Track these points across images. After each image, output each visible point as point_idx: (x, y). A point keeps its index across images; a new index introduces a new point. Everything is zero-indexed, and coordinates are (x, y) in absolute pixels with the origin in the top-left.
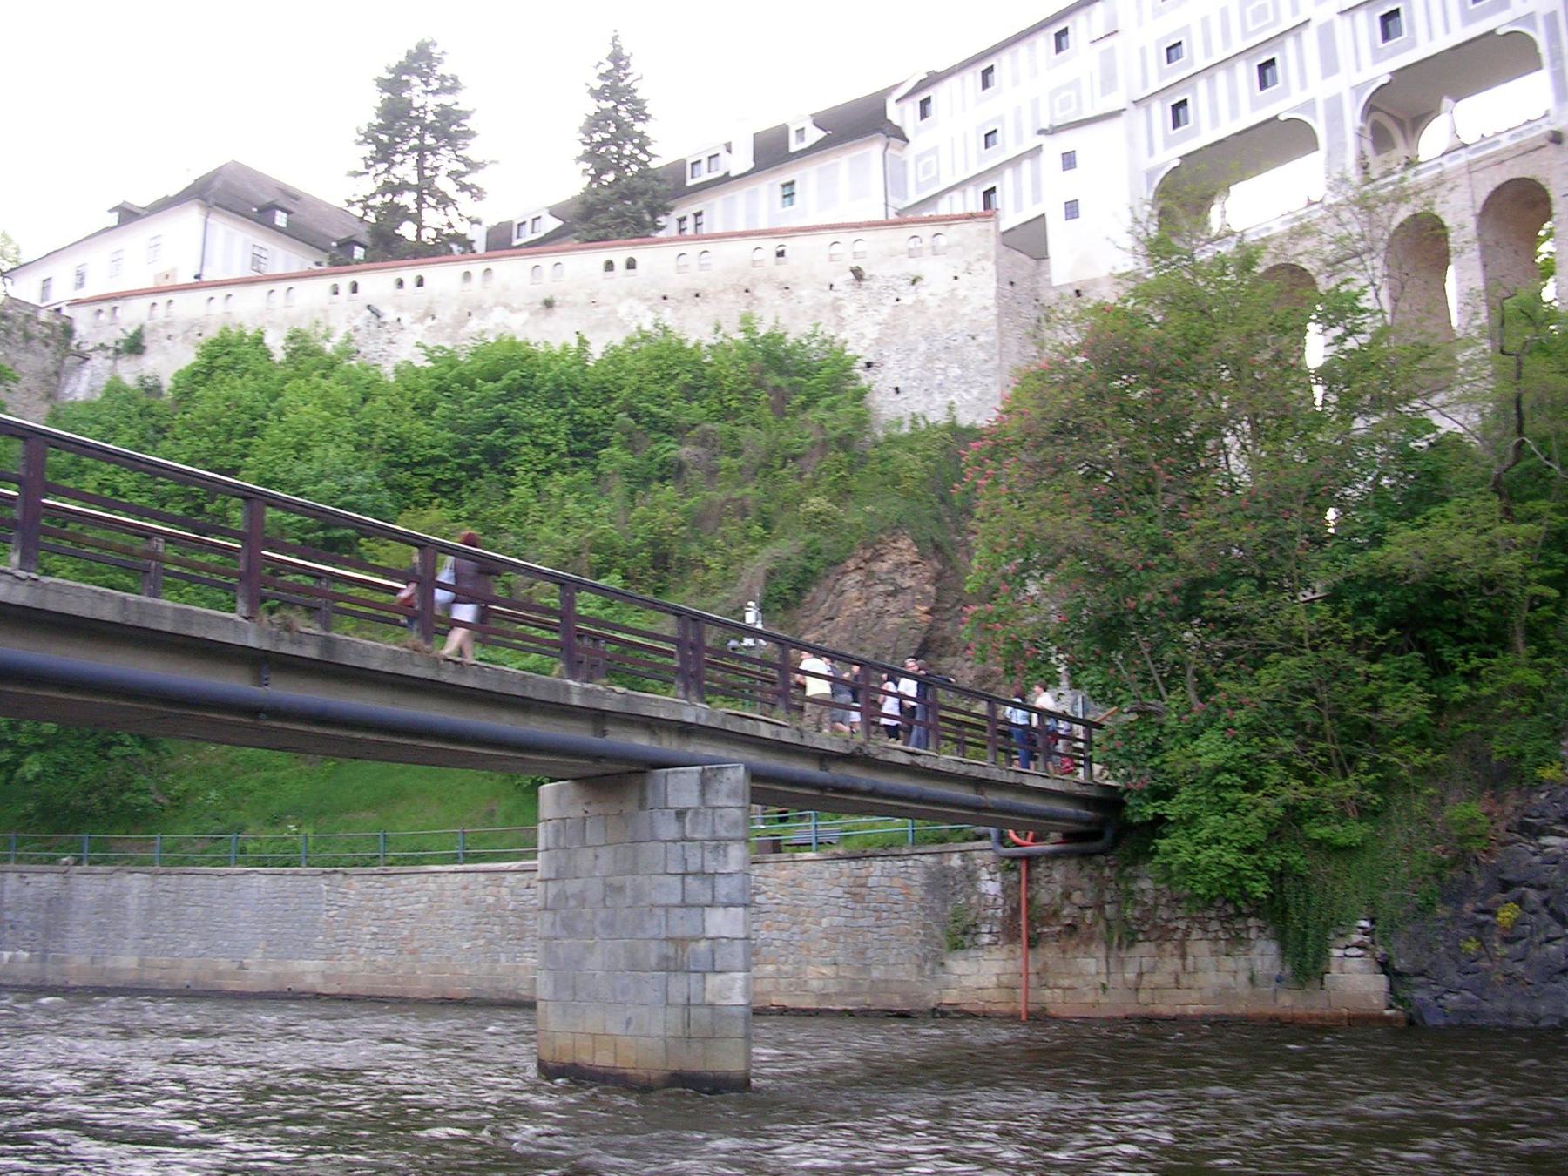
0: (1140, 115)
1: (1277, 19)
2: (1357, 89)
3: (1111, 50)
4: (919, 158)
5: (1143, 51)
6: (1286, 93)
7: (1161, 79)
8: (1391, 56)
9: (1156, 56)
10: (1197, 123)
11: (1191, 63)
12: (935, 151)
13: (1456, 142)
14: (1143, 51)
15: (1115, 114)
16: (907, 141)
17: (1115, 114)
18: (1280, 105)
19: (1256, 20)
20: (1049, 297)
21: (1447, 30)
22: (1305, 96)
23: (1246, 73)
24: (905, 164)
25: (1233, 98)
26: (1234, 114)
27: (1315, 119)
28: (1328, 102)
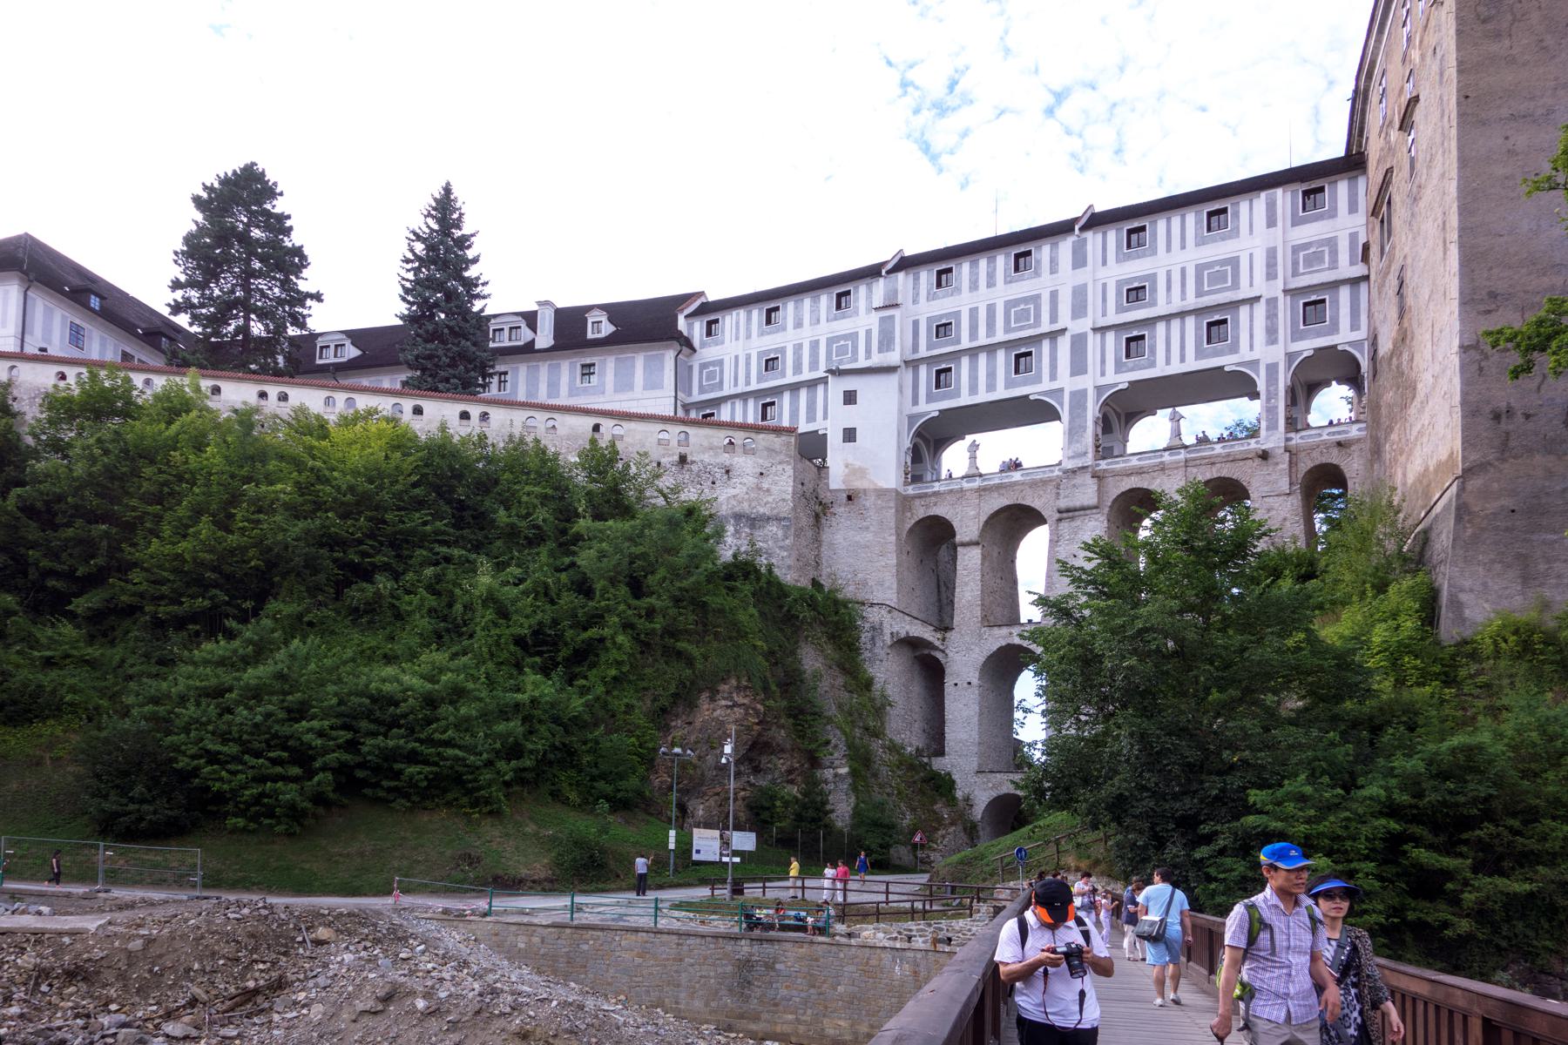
1: (1037, 322)
3: (892, 317)
7: (928, 349)
8: (1132, 370)
21: (1183, 360)
22: (1055, 385)
25: (991, 375)
26: (991, 387)
27: (1062, 405)
28: (1073, 394)
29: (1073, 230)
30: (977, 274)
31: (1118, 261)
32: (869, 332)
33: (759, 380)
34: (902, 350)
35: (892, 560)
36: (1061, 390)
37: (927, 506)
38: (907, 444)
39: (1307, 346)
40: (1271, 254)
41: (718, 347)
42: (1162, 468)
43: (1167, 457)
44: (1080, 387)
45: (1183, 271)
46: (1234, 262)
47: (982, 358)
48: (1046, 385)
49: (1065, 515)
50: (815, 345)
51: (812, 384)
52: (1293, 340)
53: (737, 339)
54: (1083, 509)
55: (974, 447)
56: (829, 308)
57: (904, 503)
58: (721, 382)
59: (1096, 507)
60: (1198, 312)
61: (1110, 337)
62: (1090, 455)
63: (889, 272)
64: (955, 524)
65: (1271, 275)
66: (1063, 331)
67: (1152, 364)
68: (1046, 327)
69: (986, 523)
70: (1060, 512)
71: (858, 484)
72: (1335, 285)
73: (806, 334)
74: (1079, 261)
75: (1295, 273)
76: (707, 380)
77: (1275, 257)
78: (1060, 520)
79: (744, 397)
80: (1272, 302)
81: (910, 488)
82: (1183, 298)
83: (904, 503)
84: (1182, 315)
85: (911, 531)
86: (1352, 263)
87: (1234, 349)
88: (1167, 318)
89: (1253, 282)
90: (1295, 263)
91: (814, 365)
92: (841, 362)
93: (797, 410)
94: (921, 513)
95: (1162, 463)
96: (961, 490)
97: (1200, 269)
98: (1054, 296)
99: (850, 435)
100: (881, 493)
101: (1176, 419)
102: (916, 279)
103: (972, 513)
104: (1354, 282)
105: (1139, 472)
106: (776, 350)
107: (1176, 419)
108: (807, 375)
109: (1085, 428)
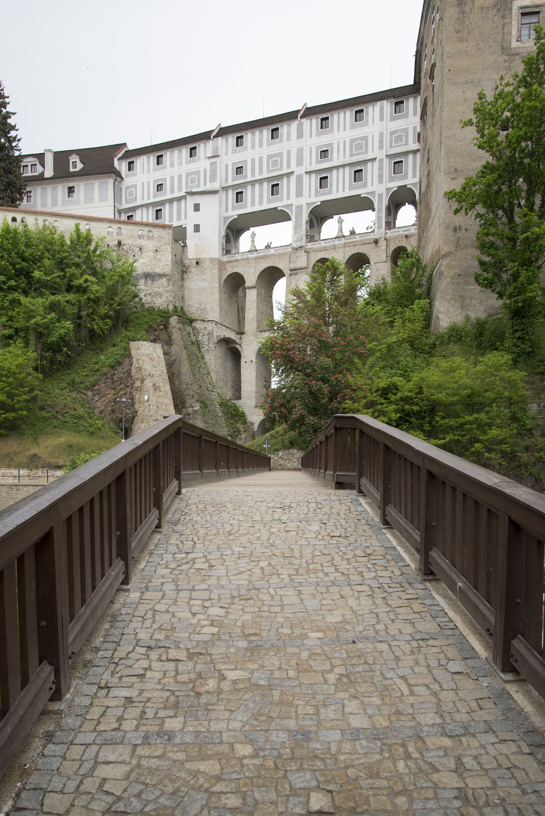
0: (223, 194)
1: (281, 169)
2: (308, 204)
3: (215, 163)
4: (127, 188)
5: (227, 166)
6: (281, 199)
7: (233, 181)
8: (322, 195)
9: (231, 171)
10: (246, 203)
11: (246, 177)
12: (135, 186)
13: (340, 234)
14: (227, 166)
15: (215, 192)
16: (123, 179)
17: (215, 192)
18: (279, 204)
19: (272, 166)
20: (186, 262)
21: (344, 190)
22: (289, 202)
23: (266, 187)
24: (121, 189)
25: (261, 196)
26: (261, 203)
27: (292, 213)
28: (297, 207)
29: (297, 117)
30: (254, 140)
31: (317, 135)
32: (205, 170)
33: (154, 196)
34: (221, 181)
35: (217, 296)
36: (292, 205)
37: (232, 267)
38: (224, 233)
39: (395, 185)
40: (381, 135)
41: (134, 177)
42: (334, 247)
43: (336, 242)
44: (300, 204)
45: (345, 142)
46: (366, 139)
47: (257, 186)
48: (285, 202)
49: (293, 272)
50: (180, 177)
51: (179, 199)
52: (390, 182)
53: (143, 173)
54: (301, 269)
55: (254, 235)
56: (186, 156)
57: (222, 265)
58: (136, 197)
59: (306, 268)
60: (350, 165)
61: (313, 176)
62: (304, 240)
63: (214, 137)
64: (245, 277)
65: (381, 147)
66: (293, 173)
67: (331, 192)
68: (285, 171)
69: (259, 276)
70: (291, 270)
71: (202, 256)
72: (406, 153)
73: (176, 171)
74: (300, 135)
75: (391, 147)
76: (129, 196)
77: (383, 137)
78: (291, 275)
79: (147, 206)
80: (381, 161)
81: (225, 257)
82: (344, 158)
83: (222, 265)
84: (343, 166)
85: (225, 280)
86: (414, 142)
87: (365, 186)
88: (337, 167)
89: (374, 151)
90: (391, 141)
91: (180, 189)
92: (192, 187)
93: (172, 213)
94: (230, 271)
95: (334, 245)
96: (248, 259)
97: (352, 141)
98: (289, 152)
99: (197, 228)
100: (212, 260)
101: (340, 221)
102: (227, 141)
103: (253, 271)
104: (415, 152)
105: (325, 249)
106: (162, 179)
107: (340, 221)
108: (177, 194)
109: (302, 225)
